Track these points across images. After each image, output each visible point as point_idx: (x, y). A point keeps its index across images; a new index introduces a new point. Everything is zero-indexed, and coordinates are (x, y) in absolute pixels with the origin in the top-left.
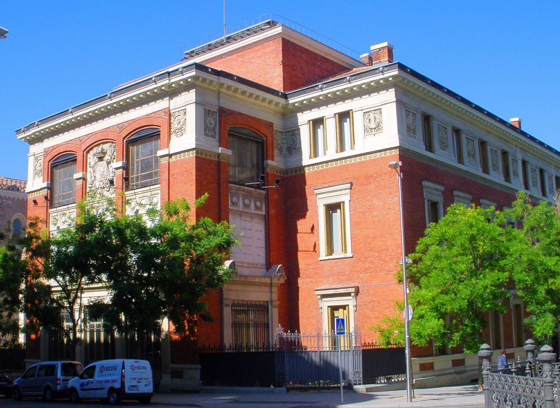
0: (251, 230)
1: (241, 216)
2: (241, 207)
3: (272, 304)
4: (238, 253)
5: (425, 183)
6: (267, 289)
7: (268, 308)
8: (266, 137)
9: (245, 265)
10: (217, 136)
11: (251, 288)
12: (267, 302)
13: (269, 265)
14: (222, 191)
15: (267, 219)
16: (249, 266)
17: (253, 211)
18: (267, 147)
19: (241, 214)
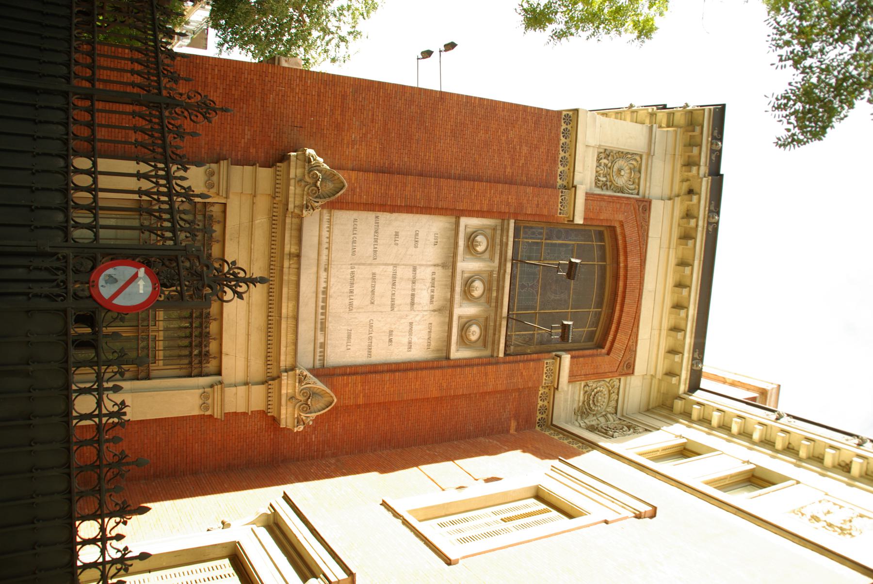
0: (412, 304)
1: (444, 266)
2: (467, 265)
3: (212, 386)
6: (257, 368)
7: (200, 375)
8: (608, 354)
9: (323, 275)
10: (598, 191)
12: (219, 373)
13: (325, 373)
14: (500, 186)
15: (441, 362)
16: (321, 296)
18: (592, 356)
19: (450, 264)
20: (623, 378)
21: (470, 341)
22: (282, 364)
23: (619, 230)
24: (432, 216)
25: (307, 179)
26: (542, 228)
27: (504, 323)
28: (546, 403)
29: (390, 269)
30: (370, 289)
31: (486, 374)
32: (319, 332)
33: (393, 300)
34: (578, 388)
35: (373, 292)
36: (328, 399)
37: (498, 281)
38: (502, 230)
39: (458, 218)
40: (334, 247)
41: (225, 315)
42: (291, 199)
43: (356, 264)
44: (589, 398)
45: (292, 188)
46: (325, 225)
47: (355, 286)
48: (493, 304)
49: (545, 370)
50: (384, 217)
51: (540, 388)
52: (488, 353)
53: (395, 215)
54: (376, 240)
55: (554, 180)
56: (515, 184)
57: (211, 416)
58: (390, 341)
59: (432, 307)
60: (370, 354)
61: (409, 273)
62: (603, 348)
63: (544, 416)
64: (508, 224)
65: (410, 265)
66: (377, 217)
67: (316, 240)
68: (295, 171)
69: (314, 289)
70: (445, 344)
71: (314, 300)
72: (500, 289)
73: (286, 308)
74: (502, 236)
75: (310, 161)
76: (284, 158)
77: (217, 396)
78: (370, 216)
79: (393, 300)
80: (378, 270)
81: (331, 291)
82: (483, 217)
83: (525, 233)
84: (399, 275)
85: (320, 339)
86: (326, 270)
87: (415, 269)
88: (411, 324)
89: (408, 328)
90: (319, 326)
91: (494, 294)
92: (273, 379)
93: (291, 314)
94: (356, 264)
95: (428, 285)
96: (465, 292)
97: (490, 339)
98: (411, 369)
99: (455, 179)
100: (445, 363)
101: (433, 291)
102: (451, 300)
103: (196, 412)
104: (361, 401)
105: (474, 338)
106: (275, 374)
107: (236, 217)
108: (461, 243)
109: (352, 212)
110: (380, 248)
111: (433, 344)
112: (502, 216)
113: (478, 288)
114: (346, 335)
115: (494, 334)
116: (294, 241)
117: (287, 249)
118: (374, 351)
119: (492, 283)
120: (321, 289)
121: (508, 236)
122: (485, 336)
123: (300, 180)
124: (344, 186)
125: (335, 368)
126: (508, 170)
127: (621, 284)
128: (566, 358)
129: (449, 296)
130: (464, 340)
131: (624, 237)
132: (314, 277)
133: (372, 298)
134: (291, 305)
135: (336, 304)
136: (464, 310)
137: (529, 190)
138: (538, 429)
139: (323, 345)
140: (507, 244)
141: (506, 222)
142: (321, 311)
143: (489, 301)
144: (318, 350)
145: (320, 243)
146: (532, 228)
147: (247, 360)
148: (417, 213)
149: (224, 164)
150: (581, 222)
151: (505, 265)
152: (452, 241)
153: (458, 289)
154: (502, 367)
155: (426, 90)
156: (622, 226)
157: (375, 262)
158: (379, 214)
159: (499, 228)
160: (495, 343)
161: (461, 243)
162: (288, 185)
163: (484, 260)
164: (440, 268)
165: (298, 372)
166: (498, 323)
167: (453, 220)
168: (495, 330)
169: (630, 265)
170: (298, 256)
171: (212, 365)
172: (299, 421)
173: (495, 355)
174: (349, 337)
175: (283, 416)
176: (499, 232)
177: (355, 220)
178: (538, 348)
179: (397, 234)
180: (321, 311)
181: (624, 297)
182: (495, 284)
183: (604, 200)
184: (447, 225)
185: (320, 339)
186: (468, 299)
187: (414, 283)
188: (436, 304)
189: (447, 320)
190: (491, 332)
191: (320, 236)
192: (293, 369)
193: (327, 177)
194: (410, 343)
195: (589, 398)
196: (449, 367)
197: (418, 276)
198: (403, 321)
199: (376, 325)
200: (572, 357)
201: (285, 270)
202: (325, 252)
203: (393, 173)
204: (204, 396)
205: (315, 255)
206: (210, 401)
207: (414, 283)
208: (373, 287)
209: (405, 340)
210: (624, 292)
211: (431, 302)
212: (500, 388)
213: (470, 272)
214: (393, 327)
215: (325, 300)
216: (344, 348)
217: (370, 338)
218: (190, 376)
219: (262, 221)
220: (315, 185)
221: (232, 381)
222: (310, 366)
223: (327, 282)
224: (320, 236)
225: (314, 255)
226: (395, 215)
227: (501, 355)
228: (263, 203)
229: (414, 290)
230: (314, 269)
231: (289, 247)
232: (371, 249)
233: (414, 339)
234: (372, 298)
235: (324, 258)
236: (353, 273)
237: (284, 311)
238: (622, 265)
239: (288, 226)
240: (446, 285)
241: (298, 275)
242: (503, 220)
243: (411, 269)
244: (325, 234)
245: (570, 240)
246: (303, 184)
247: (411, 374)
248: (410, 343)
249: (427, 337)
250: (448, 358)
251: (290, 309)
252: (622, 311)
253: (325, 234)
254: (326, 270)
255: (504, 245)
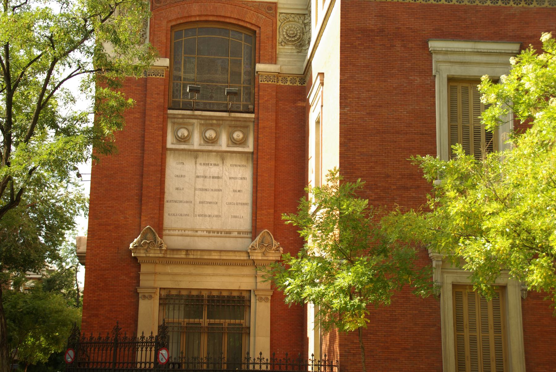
0: (218, 178)
1: (196, 157)
2: (196, 142)
3: (256, 295)
4: (187, 215)
5: (433, 45)
6: (248, 270)
9: (199, 233)
11: (209, 270)
12: (250, 291)
13: (255, 232)
14: (147, 123)
15: (255, 158)
16: (211, 234)
17: (224, 148)
19: (195, 154)
20: (279, 11)
21: (243, 138)
22: (246, 258)
23: (173, 23)
24: (167, 166)
25: (146, 247)
26: (174, 83)
27: (233, 115)
28: (289, 79)
29: (197, 192)
30: (209, 204)
31: (264, 128)
32: (232, 235)
33: (216, 190)
34: (282, 51)
35: (210, 203)
36: (266, 234)
37: (206, 119)
38: (174, 118)
39: (167, 149)
40: (184, 227)
41: (219, 288)
42: (157, 255)
43: (194, 214)
44: (290, 41)
45: (151, 255)
46: (172, 232)
47: (206, 214)
48: (221, 122)
49: (266, 82)
50: (167, 197)
51: (278, 84)
52: (251, 125)
53: (166, 190)
54: (181, 202)
55: (141, 86)
56: (145, 110)
57: (272, 296)
58: (239, 191)
59: (221, 165)
60: (246, 204)
61: (200, 180)
62: (255, 32)
63: (298, 80)
64: (171, 114)
65: (195, 180)
66: (167, 202)
67: (180, 238)
68: (141, 254)
69: (207, 238)
70: (244, 155)
71: (213, 238)
72: (211, 118)
73: (215, 256)
74: (178, 118)
75: (136, 246)
76: (135, 258)
77: (261, 293)
78: (167, 205)
79: (216, 190)
80: (198, 200)
81: (209, 228)
82: (166, 133)
83: (177, 97)
84: (200, 187)
85: (235, 234)
86: (197, 231)
87: (198, 177)
88: (230, 178)
89: (233, 180)
90: (228, 235)
91: (215, 122)
92: (254, 262)
93: (219, 254)
94: (194, 214)
95: (207, 167)
96: (212, 143)
97: (243, 124)
98: (257, 179)
99: (143, 153)
100: (255, 156)
101: (211, 164)
102: (217, 152)
103: (269, 304)
104: (272, 211)
105: (241, 136)
106: (252, 262)
107: (167, 283)
108: (182, 147)
109: (165, 217)
110: (185, 199)
111: (244, 163)
112: (165, 118)
113: (211, 134)
114: (234, 219)
115: (240, 121)
116: (179, 253)
117: (184, 256)
118: (245, 201)
119: (208, 124)
120: (207, 234)
121: (178, 114)
122: (241, 127)
123: (146, 250)
124: (149, 228)
125: (252, 226)
126: (136, 115)
127: (211, 19)
128: (260, 67)
129: (215, 153)
130: (242, 142)
131: (178, 19)
132: (200, 239)
133: (214, 203)
134: (213, 254)
135: (216, 225)
136: (223, 144)
137: (148, 100)
138: (305, 85)
139: (239, 233)
140: (183, 115)
141: (169, 116)
142: (220, 234)
143: (219, 125)
144: (242, 235)
145: (182, 235)
146: (173, 92)
147: (244, 276)
148: (164, 178)
149: (139, 290)
150: (168, 60)
151: (196, 115)
152: (181, 152)
153: (210, 148)
154: (260, 116)
155: (92, 170)
156: (170, 21)
157: (193, 202)
158: (165, 200)
159: (173, 120)
160: (246, 120)
161: (182, 147)
162: (149, 257)
163: (193, 130)
164: (197, 160)
165: (249, 251)
166: (233, 119)
167: (168, 152)
168: (237, 121)
169: (198, 13)
170: (187, 250)
171: (245, 294)
172: (277, 250)
173: (253, 120)
174: (235, 217)
175: (274, 258)
176: (176, 120)
177: (169, 215)
178: (252, 84)
179: (177, 189)
180: (220, 234)
181: (220, 16)
182: (208, 122)
183: (153, 39)
184: (172, 156)
185: (235, 234)
186: (217, 140)
187: (206, 177)
188: (220, 162)
189: (229, 154)
190: (238, 123)
191: (178, 235)
192: (248, 253)
193: (144, 237)
194: (241, 179)
195: (290, 41)
196: (257, 153)
197: (202, 174)
198: (228, 183)
199: (229, 201)
200: (259, 63)
201: (195, 257)
202: (187, 232)
203: (142, 194)
204: (261, 299)
205: (188, 238)
206: (263, 297)
207: (206, 177)
208: (207, 203)
209: (240, 181)
210: (217, 16)
211: (218, 165)
212: (274, 117)
213: (200, 140)
214: (231, 189)
215: (214, 232)
216: (242, 220)
217: (237, 204)
218: (250, 306)
219: (169, 269)
220: (149, 243)
221: (254, 284)
222: (250, 240)
223: (203, 231)
224: (178, 235)
225: (188, 239)
226: (166, 190)
227: (253, 116)
228: (159, 268)
229: (210, 177)
230: (196, 238)
231: (183, 255)
232: (186, 205)
233: (240, 176)
234: (214, 203)
235: (190, 233)
236: (199, 216)
237: (217, 257)
238: (198, 19)
239: (172, 256)
240: (208, 156)
241: (198, 250)
242: (168, 118)
243: (198, 179)
244: (176, 232)
245: (181, 60)
246: (148, 250)
247: (259, 179)
248: (241, 179)
249: (239, 167)
250: (253, 153)
251: (216, 254)
252: (230, 18)
253: (176, 232)
254: (197, 231)
255: (184, 117)
